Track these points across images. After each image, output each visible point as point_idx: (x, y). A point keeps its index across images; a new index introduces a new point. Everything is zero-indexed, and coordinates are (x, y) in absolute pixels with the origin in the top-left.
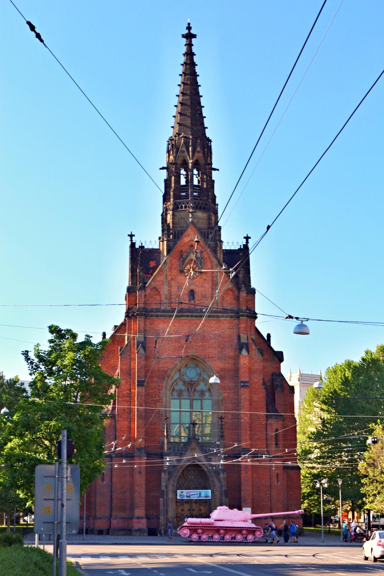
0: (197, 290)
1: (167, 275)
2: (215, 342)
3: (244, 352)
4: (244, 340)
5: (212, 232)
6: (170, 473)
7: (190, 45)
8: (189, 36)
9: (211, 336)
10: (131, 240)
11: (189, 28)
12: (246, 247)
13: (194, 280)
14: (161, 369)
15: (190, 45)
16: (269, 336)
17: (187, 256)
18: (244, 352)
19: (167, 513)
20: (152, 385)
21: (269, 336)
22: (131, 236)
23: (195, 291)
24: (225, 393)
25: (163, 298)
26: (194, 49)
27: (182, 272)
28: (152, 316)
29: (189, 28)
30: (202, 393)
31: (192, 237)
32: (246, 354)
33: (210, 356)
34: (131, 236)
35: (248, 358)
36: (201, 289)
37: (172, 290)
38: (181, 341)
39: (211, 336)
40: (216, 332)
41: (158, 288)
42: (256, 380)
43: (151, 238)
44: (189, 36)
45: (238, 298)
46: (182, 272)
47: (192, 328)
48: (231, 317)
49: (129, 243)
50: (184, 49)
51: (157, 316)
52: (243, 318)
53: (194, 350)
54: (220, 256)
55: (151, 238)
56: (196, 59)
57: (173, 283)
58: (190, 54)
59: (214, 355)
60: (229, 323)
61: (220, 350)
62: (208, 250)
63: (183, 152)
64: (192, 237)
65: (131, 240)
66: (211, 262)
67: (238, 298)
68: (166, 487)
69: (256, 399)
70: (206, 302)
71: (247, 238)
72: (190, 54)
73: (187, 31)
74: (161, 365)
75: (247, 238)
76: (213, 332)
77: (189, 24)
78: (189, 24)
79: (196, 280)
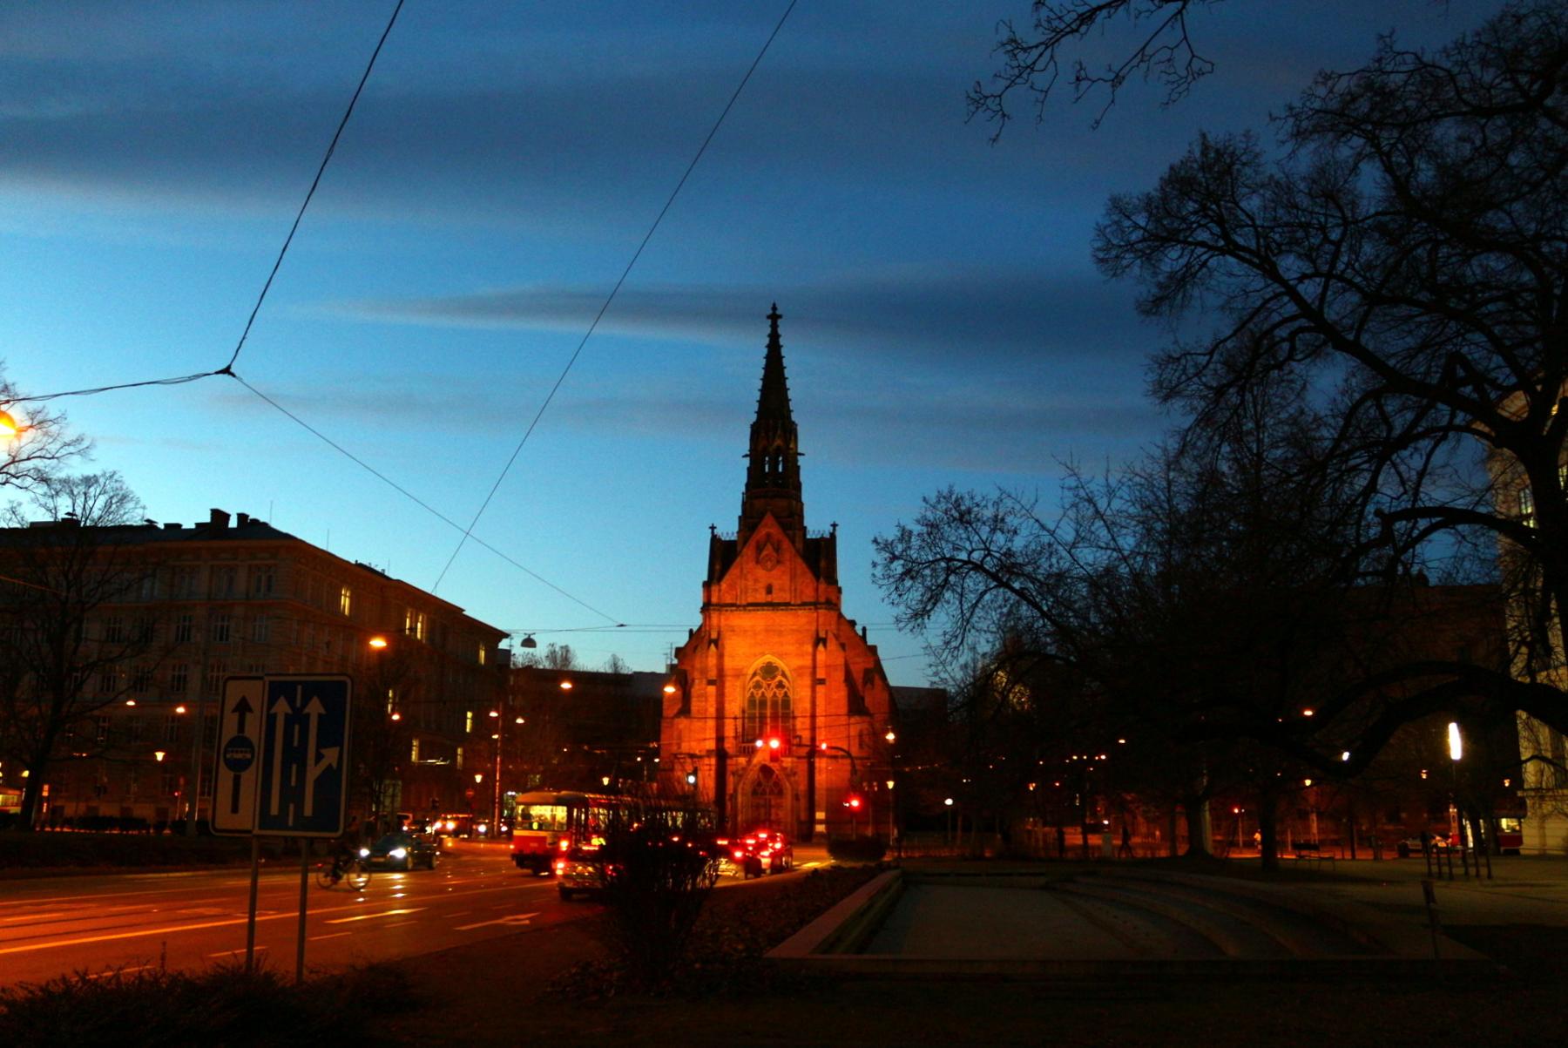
3: (821, 647)
4: (822, 635)
5: (792, 517)
7: (774, 327)
8: (774, 318)
12: (833, 536)
15: (774, 327)
16: (864, 630)
18: (821, 647)
19: (736, 816)
21: (864, 630)
22: (713, 528)
26: (780, 331)
31: (769, 527)
34: (713, 528)
43: (729, 529)
45: (817, 590)
50: (769, 330)
54: (799, 545)
55: (729, 529)
56: (782, 341)
64: (769, 527)
67: (817, 590)
68: (735, 790)
71: (834, 526)
75: (834, 526)
77: (774, 308)
78: (774, 308)
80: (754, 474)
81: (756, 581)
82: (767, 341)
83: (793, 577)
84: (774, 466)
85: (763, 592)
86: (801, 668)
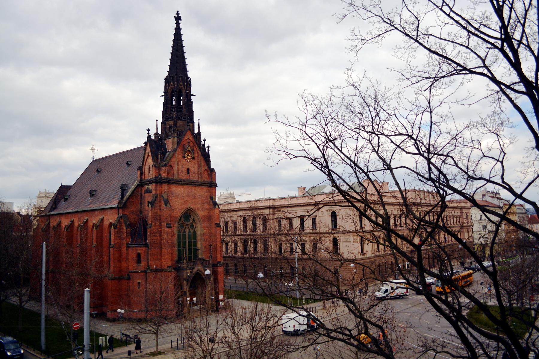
0: (191, 168)
6: (187, 281)
7: (178, 24)
8: (178, 19)
10: (148, 133)
11: (178, 14)
15: (178, 24)
22: (148, 130)
25: (175, 172)
26: (181, 26)
27: (184, 157)
29: (178, 14)
34: (148, 130)
44: (178, 19)
46: (184, 157)
49: (147, 135)
50: (175, 26)
51: (172, 183)
58: (178, 29)
63: (181, 85)
65: (148, 133)
66: (198, 153)
72: (178, 29)
73: (176, 16)
80: (167, 105)
82: (174, 31)
83: (199, 166)
84: (178, 101)
85: (185, 172)
86: (204, 216)
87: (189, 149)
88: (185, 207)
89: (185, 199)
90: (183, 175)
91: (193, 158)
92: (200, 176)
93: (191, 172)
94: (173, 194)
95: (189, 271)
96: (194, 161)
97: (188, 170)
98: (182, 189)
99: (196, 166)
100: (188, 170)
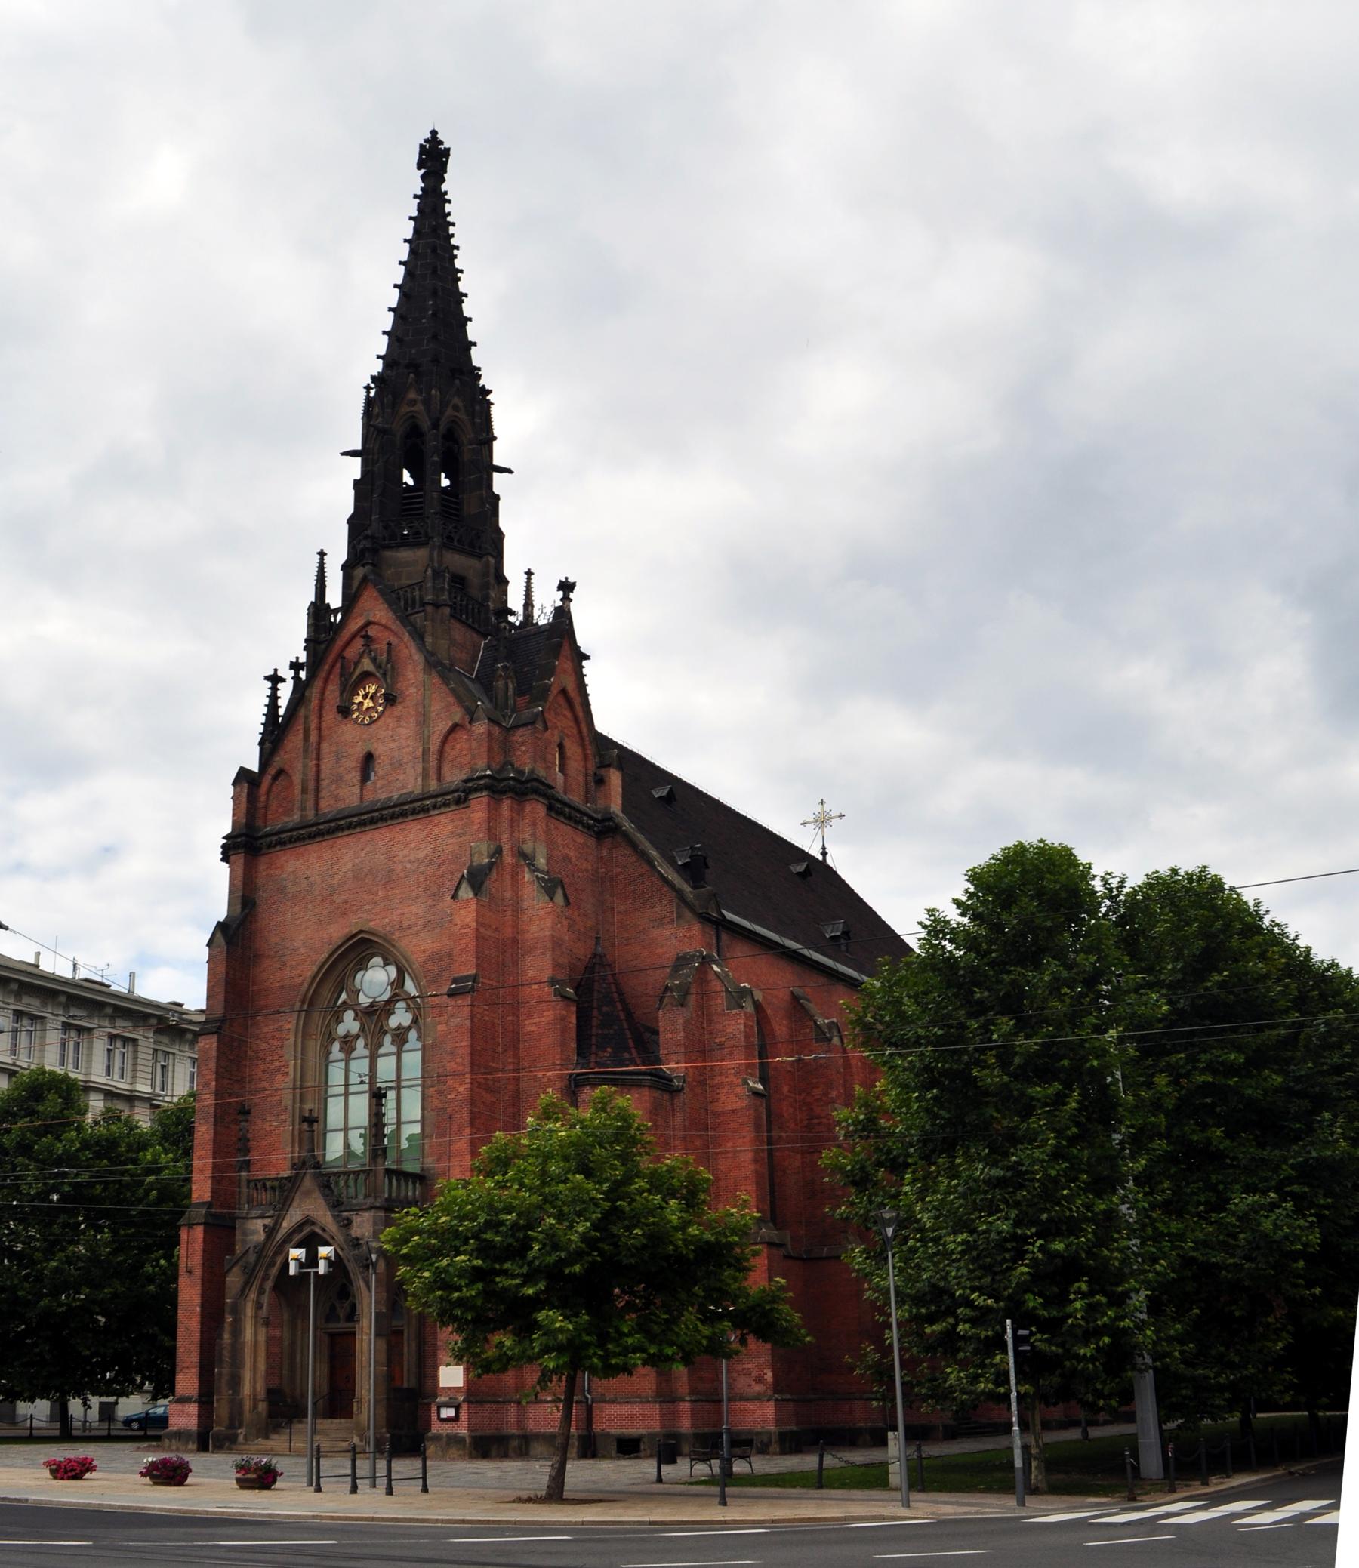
0: (379, 750)
1: (307, 732)
2: (417, 882)
9: (409, 866)
13: (374, 726)
14: (287, 983)
17: (356, 665)
20: (265, 1029)
23: (376, 754)
24: (440, 1023)
28: (270, 846)
30: (400, 1037)
32: (471, 895)
33: (405, 924)
35: (474, 907)
36: (391, 745)
37: (323, 767)
38: (335, 897)
39: (409, 866)
40: (421, 854)
41: (286, 767)
42: (532, 974)
46: (345, 711)
47: (363, 854)
48: (458, 802)
51: (282, 843)
52: (478, 795)
53: (364, 916)
57: (325, 746)
59: (414, 920)
60: (453, 821)
61: (430, 902)
62: (407, 637)
69: (533, 1028)
70: (401, 777)
74: (288, 973)
76: (412, 858)
79: (380, 723)
81: (338, 757)
86: (434, 958)
87: (367, 665)
88: (336, 932)
89: (339, 899)
90: (344, 792)
91: (390, 700)
92: (419, 768)
93: (380, 768)
94: (282, 890)
95: (258, 1225)
96: (398, 710)
97: (369, 758)
98: (327, 855)
99: (407, 731)
100: (369, 758)
